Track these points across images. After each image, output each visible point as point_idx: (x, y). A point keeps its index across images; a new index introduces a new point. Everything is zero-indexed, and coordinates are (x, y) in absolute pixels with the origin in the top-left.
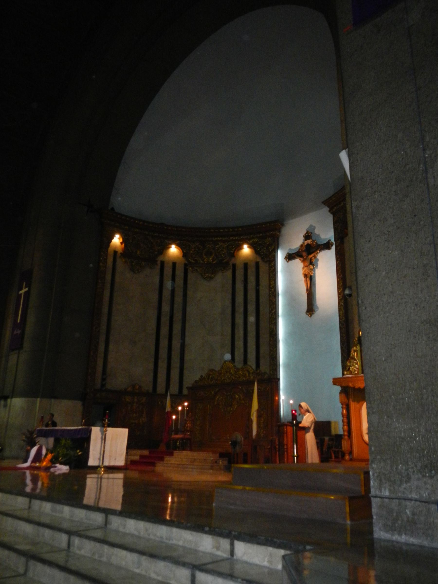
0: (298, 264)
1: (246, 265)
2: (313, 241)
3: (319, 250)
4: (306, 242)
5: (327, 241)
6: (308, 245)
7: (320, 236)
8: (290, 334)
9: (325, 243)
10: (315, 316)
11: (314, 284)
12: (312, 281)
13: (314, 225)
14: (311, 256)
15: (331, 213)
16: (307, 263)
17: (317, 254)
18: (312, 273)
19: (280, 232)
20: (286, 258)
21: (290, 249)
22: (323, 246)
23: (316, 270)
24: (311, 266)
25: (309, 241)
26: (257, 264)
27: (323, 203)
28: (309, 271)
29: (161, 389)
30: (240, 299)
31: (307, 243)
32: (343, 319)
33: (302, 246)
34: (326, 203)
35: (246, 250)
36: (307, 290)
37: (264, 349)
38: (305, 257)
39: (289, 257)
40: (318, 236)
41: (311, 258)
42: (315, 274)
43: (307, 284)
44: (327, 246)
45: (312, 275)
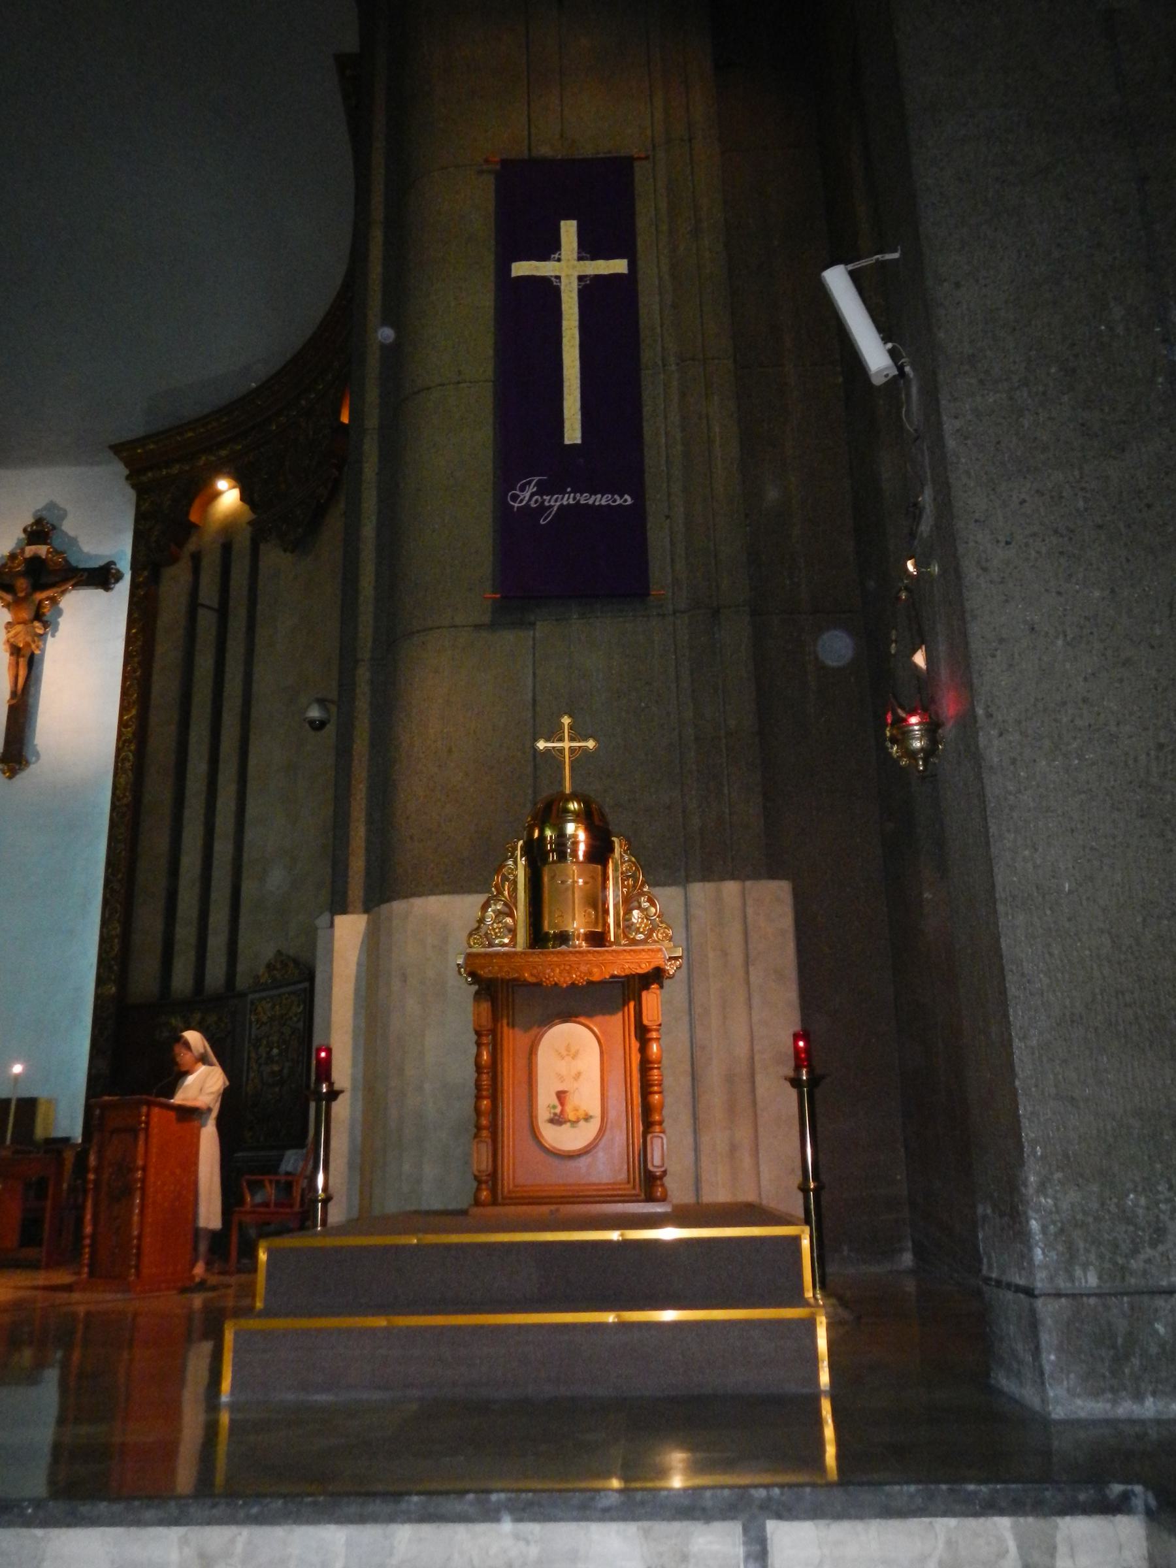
2: (57, 552)
3: (72, 583)
4: (30, 551)
5: (102, 563)
6: (36, 559)
7: (77, 542)
9: (94, 570)
10: (23, 778)
11: (38, 680)
12: (33, 673)
13: (61, 503)
14: (40, 596)
15: (133, 486)
16: (25, 615)
17: (63, 593)
18: (38, 647)
22: (86, 575)
23: (50, 639)
24: (37, 624)
25: (42, 550)
27: (112, 447)
28: (29, 639)
31: (32, 554)
32: (125, 801)
33: (13, 556)
34: (118, 449)
36: (14, 694)
38: (22, 595)
40: (73, 541)
41: (40, 602)
42: (43, 651)
43: (16, 677)
44: (103, 577)
45: (37, 652)
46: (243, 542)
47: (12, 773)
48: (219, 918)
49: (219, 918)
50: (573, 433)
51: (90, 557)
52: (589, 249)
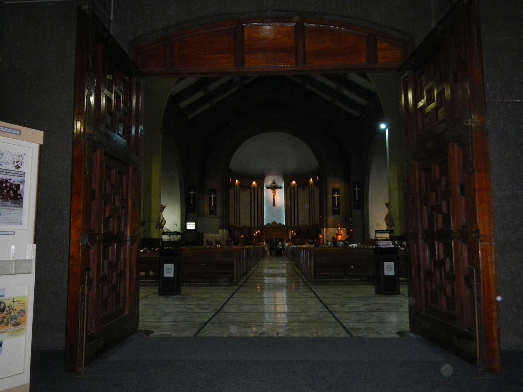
0: (270, 191)
1: (254, 188)
2: (276, 185)
4: (274, 185)
8: (267, 211)
13: (275, 179)
19: (264, 179)
20: (266, 188)
21: (267, 185)
25: (275, 185)
26: (257, 188)
29: (236, 226)
30: (253, 198)
35: (254, 183)
37: (260, 214)
39: (268, 188)
40: (276, 183)
44: (281, 188)
46: (296, 187)
47: (274, 206)
48: (296, 221)
49: (296, 221)
50: (336, 205)
51: (279, 185)
52: (337, 194)
